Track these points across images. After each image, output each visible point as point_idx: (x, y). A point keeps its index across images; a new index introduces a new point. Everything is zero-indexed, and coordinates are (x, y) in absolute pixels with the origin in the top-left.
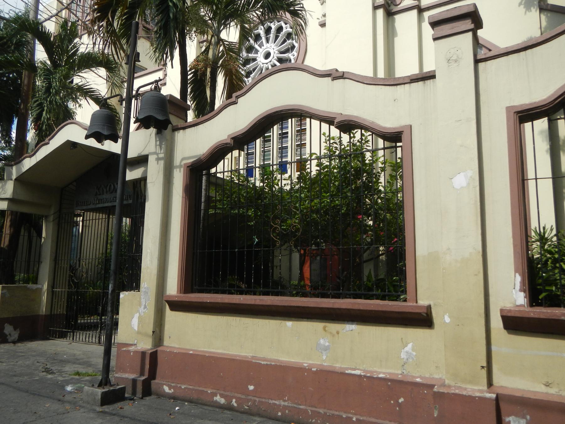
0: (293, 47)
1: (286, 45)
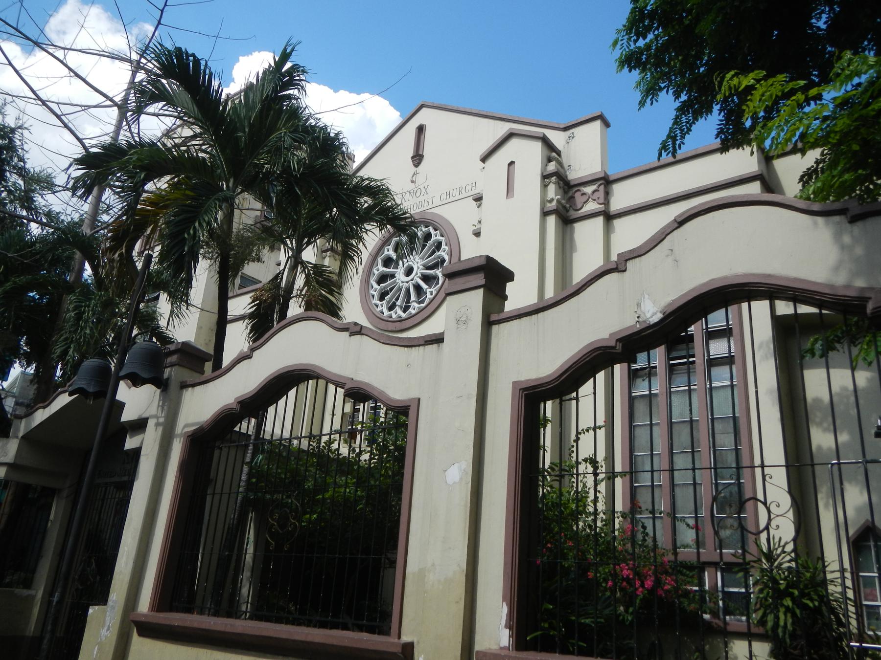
1: (434, 259)
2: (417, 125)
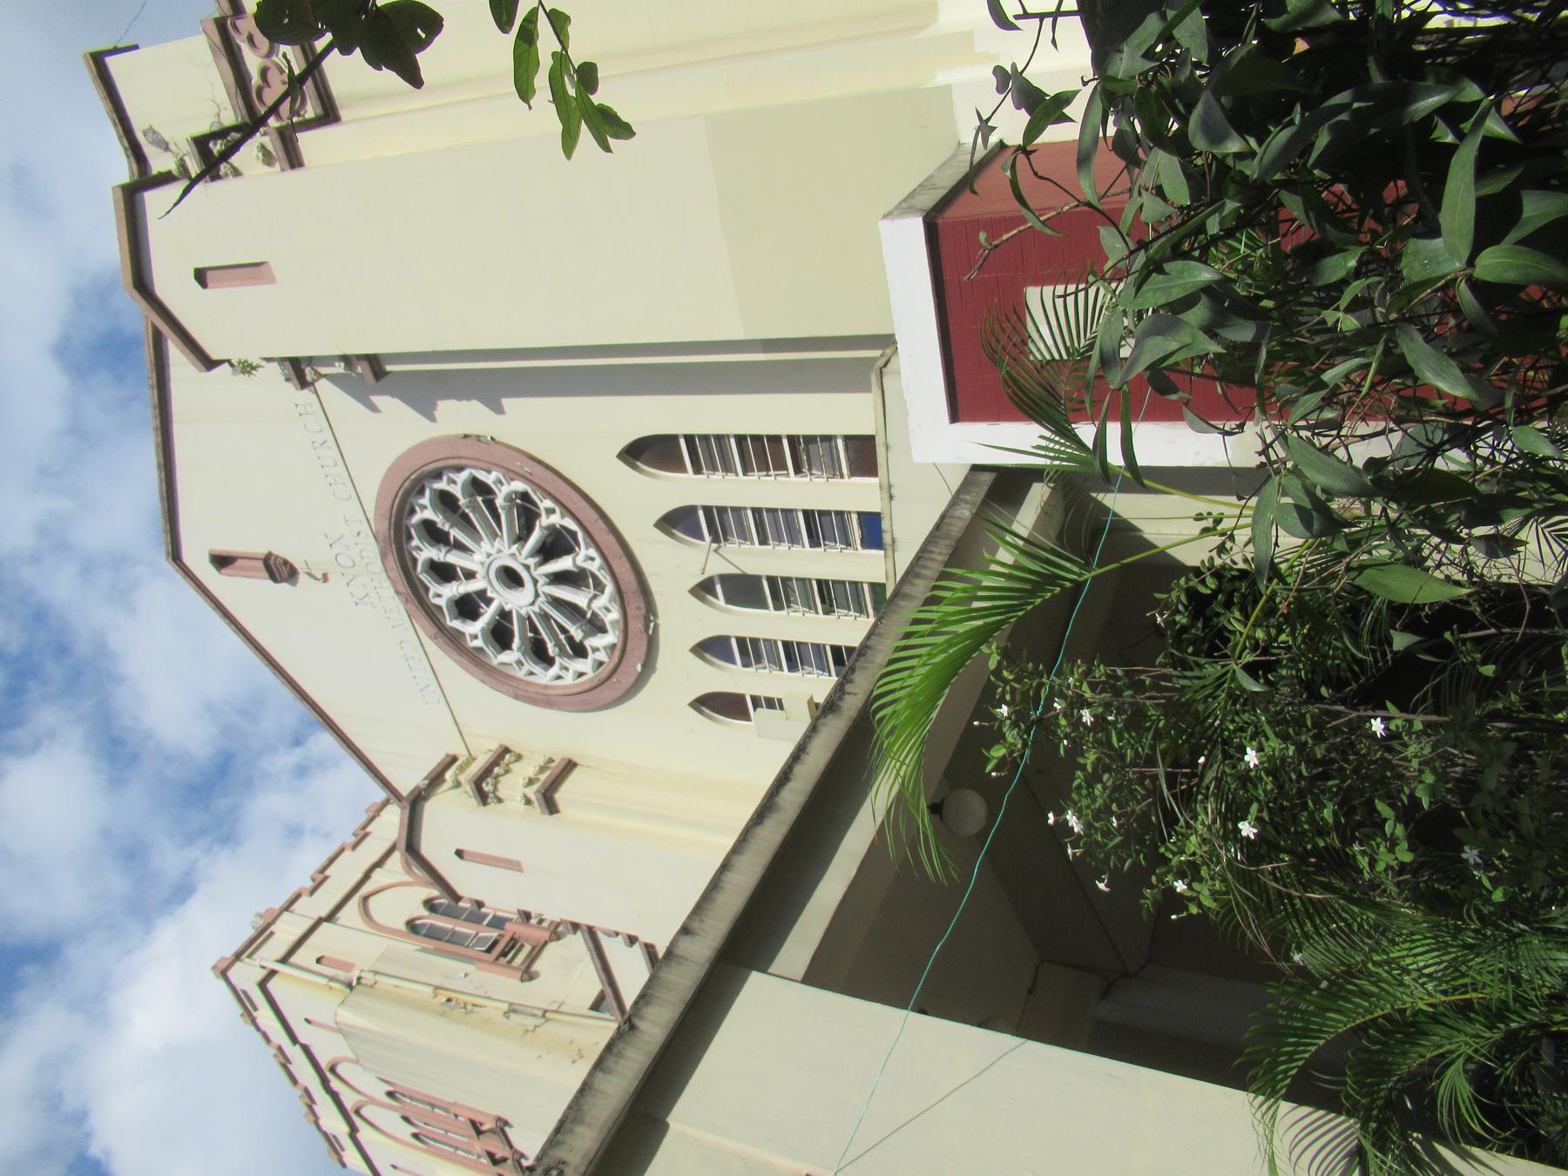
0: (478, 487)
2: (212, 569)
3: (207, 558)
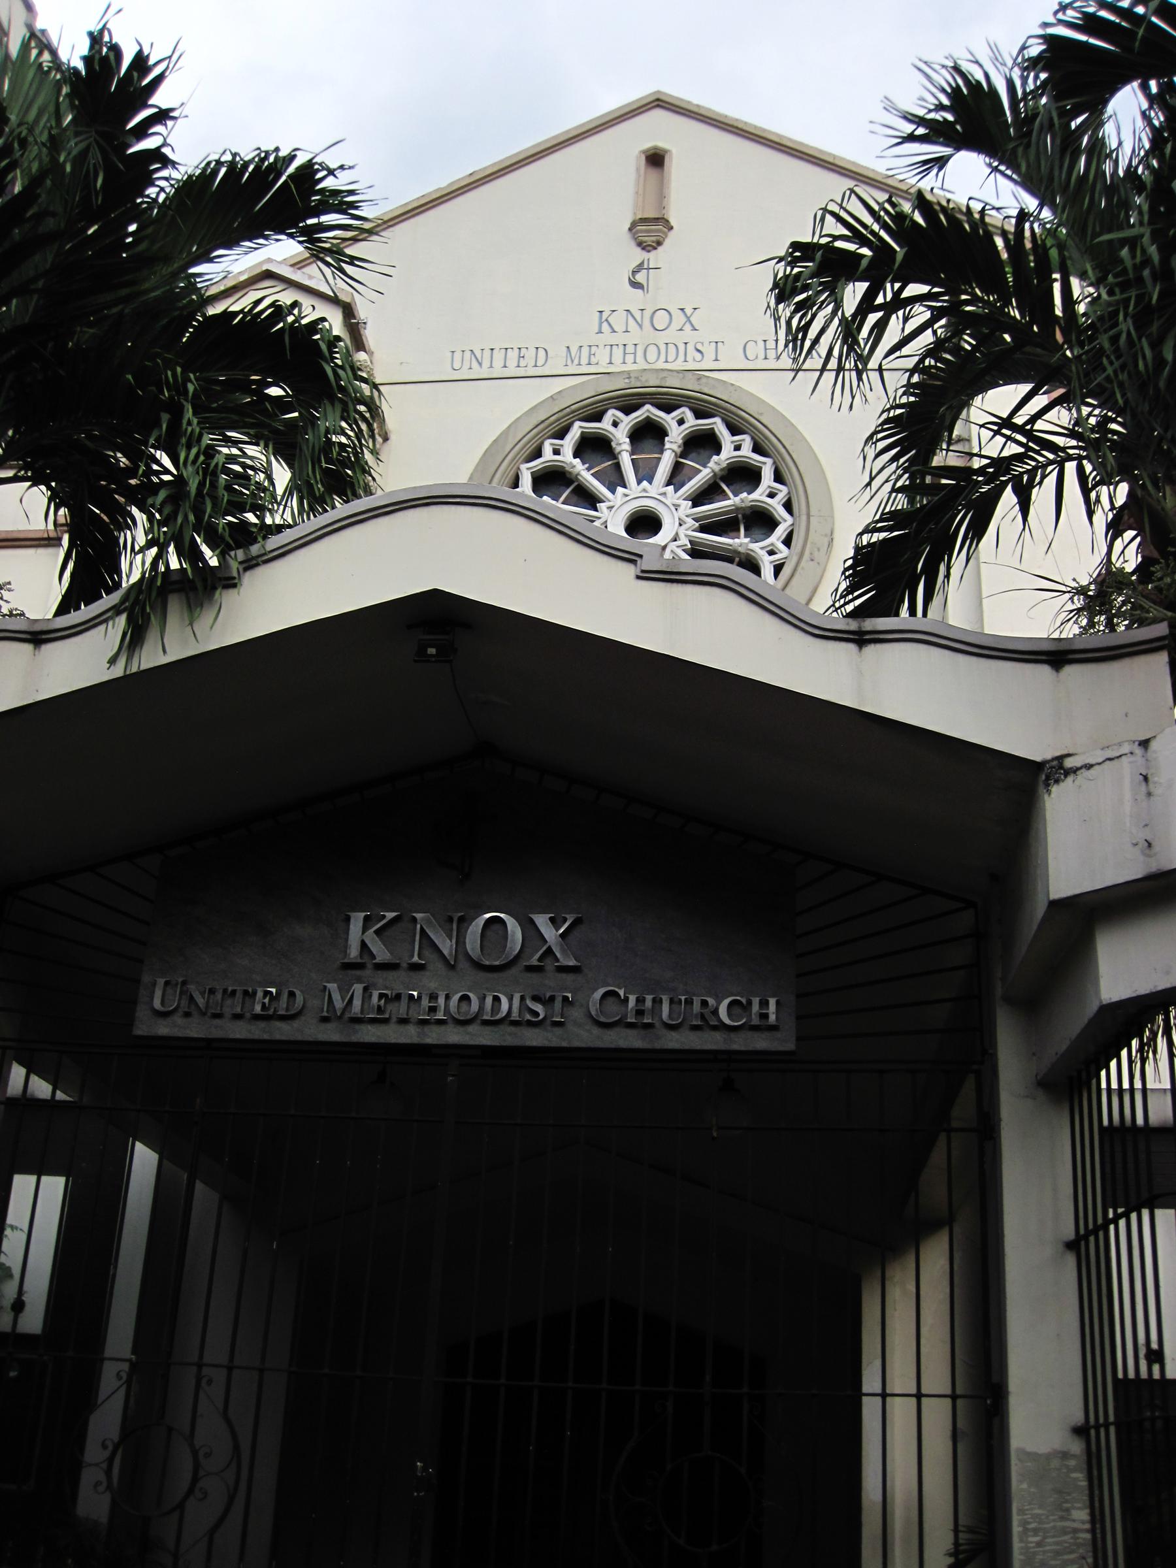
3: (662, 144)
